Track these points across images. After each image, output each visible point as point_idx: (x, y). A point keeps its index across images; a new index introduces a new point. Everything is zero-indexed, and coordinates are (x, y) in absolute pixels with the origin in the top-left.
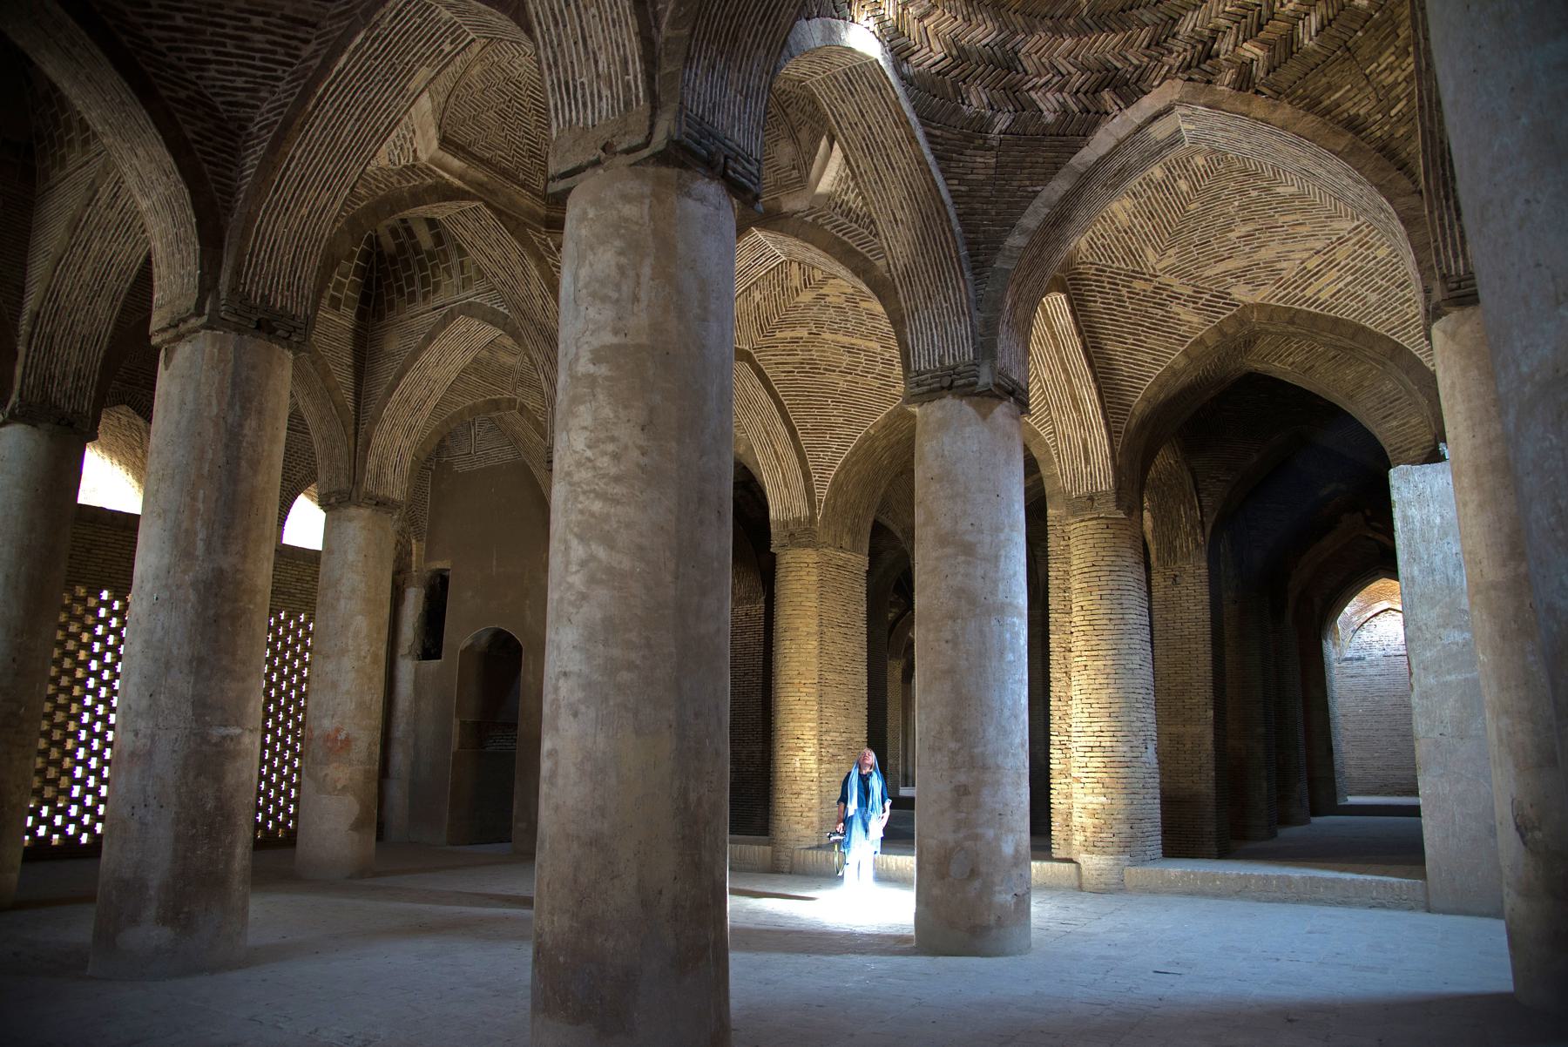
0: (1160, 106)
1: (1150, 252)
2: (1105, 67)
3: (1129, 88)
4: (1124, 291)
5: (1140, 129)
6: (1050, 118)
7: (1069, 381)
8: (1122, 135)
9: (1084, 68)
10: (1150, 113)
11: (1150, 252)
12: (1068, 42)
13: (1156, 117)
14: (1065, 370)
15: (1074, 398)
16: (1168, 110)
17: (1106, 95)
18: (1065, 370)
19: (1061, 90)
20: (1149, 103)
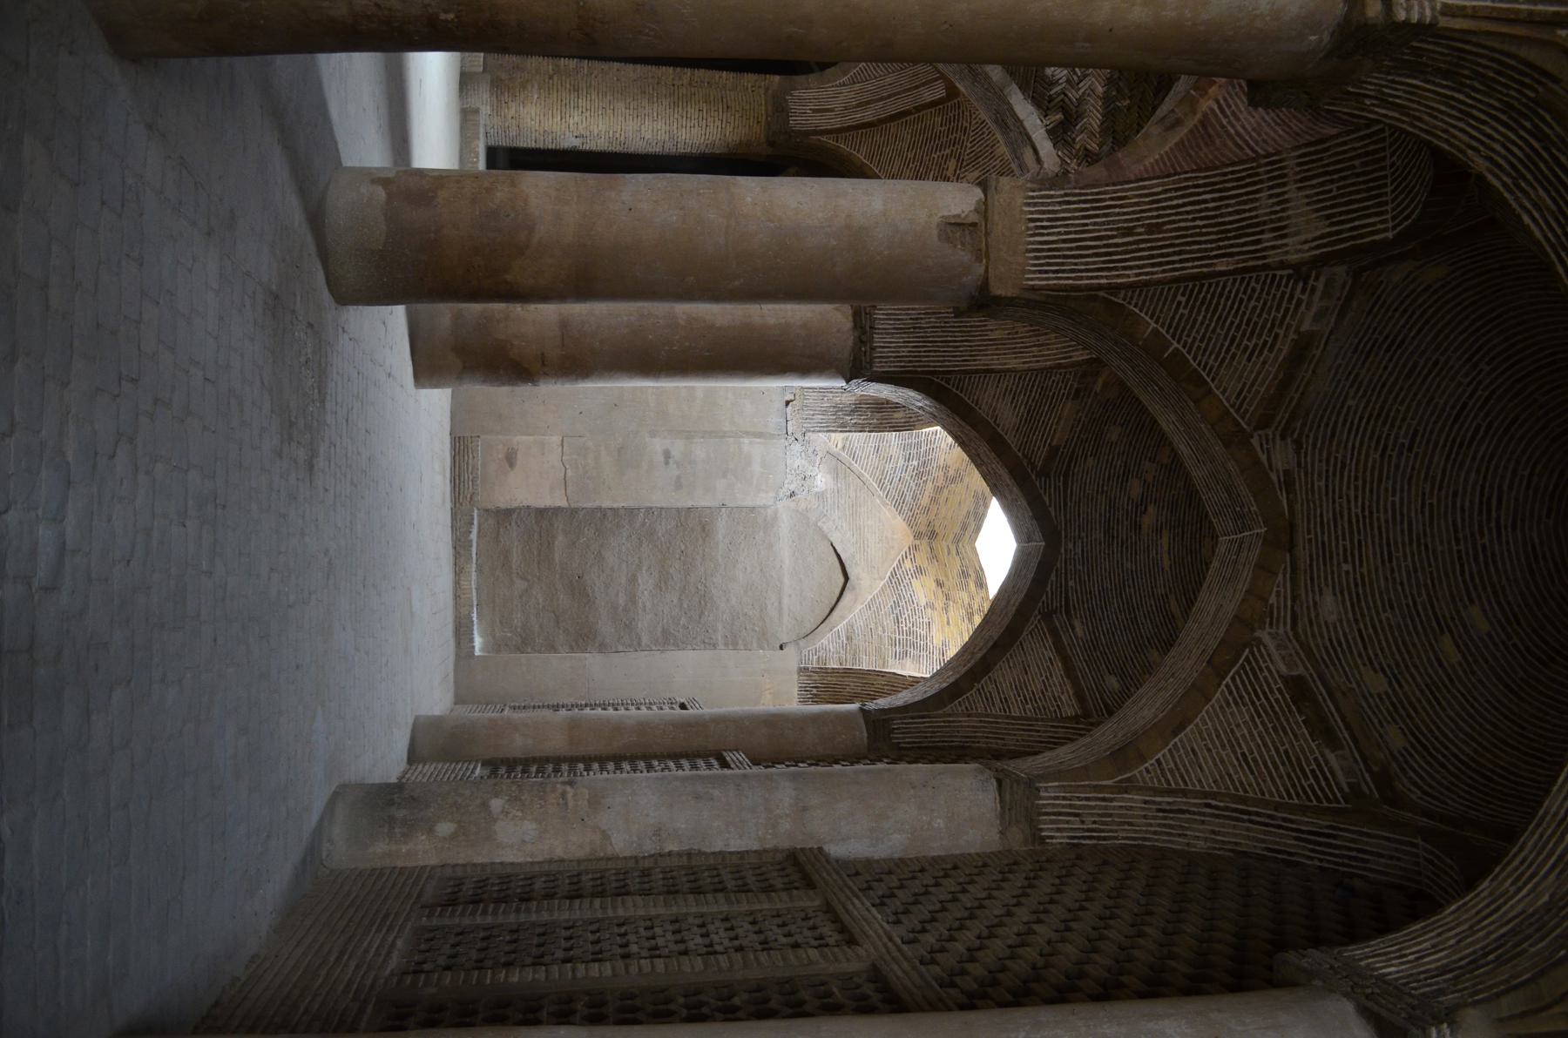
0: (1042, 153)
1: (976, 174)
2: (1080, 116)
3: (1059, 134)
4: (948, 151)
5: (1029, 138)
6: (1049, 71)
7: (881, 99)
8: (1026, 124)
9: (1081, 101)
10: (1038, 147)
11: (976, 174)
12: (1100, 90)
13: (1036, 151)
14: (889, 96)
15: (868, 103)
16: (1039, 160)
17: (1059, 116)
18: (889, 96)
19: (1068, 81)
20: (1045, 147)
